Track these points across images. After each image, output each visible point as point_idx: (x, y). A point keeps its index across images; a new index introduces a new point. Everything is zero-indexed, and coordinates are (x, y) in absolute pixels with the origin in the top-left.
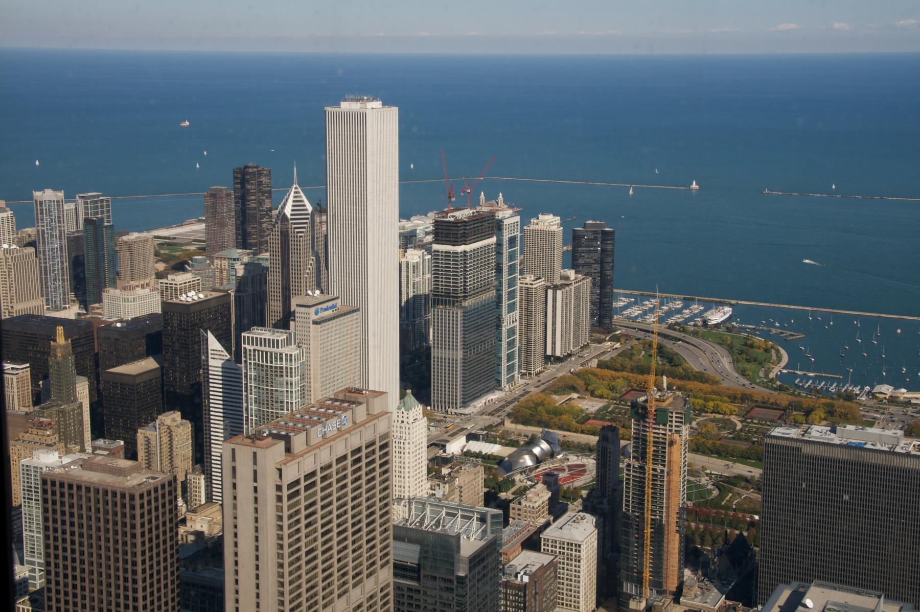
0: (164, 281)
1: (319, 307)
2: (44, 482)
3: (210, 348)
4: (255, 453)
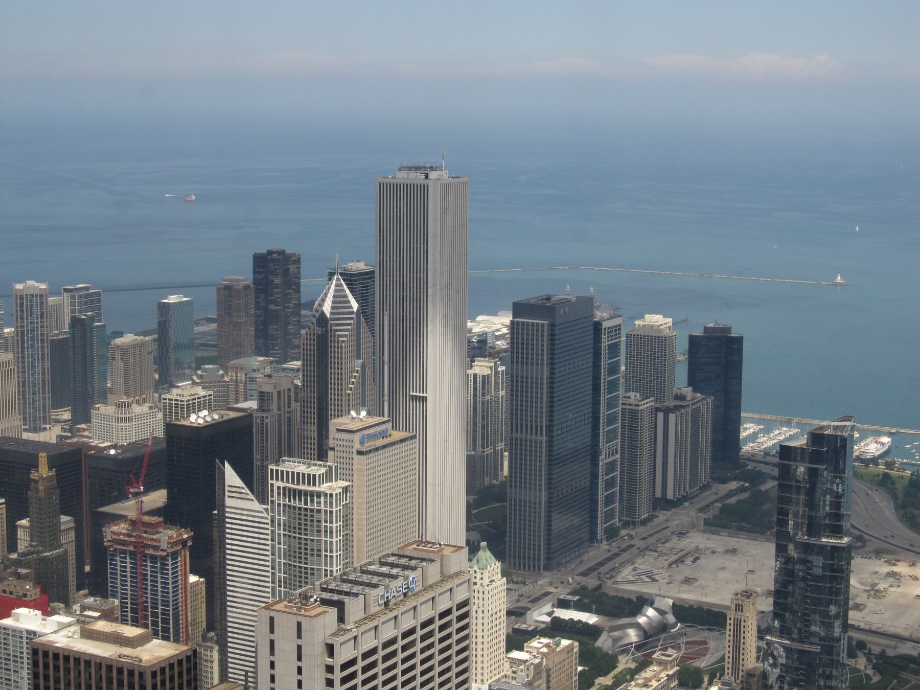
0: (168, 396)
1: (366, 432)
2: (35, 652)
3: (227, 483)
4: (299, 624)
